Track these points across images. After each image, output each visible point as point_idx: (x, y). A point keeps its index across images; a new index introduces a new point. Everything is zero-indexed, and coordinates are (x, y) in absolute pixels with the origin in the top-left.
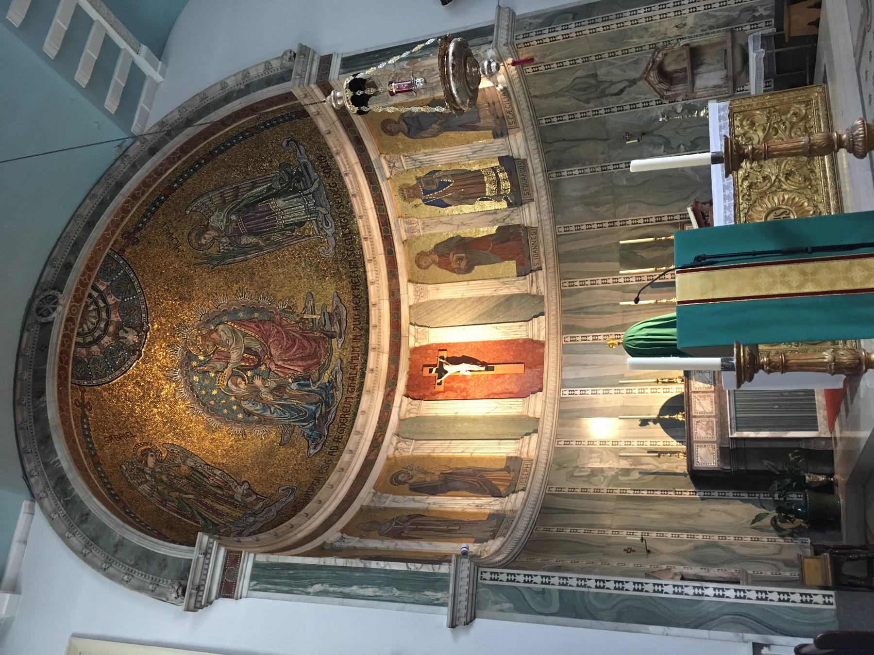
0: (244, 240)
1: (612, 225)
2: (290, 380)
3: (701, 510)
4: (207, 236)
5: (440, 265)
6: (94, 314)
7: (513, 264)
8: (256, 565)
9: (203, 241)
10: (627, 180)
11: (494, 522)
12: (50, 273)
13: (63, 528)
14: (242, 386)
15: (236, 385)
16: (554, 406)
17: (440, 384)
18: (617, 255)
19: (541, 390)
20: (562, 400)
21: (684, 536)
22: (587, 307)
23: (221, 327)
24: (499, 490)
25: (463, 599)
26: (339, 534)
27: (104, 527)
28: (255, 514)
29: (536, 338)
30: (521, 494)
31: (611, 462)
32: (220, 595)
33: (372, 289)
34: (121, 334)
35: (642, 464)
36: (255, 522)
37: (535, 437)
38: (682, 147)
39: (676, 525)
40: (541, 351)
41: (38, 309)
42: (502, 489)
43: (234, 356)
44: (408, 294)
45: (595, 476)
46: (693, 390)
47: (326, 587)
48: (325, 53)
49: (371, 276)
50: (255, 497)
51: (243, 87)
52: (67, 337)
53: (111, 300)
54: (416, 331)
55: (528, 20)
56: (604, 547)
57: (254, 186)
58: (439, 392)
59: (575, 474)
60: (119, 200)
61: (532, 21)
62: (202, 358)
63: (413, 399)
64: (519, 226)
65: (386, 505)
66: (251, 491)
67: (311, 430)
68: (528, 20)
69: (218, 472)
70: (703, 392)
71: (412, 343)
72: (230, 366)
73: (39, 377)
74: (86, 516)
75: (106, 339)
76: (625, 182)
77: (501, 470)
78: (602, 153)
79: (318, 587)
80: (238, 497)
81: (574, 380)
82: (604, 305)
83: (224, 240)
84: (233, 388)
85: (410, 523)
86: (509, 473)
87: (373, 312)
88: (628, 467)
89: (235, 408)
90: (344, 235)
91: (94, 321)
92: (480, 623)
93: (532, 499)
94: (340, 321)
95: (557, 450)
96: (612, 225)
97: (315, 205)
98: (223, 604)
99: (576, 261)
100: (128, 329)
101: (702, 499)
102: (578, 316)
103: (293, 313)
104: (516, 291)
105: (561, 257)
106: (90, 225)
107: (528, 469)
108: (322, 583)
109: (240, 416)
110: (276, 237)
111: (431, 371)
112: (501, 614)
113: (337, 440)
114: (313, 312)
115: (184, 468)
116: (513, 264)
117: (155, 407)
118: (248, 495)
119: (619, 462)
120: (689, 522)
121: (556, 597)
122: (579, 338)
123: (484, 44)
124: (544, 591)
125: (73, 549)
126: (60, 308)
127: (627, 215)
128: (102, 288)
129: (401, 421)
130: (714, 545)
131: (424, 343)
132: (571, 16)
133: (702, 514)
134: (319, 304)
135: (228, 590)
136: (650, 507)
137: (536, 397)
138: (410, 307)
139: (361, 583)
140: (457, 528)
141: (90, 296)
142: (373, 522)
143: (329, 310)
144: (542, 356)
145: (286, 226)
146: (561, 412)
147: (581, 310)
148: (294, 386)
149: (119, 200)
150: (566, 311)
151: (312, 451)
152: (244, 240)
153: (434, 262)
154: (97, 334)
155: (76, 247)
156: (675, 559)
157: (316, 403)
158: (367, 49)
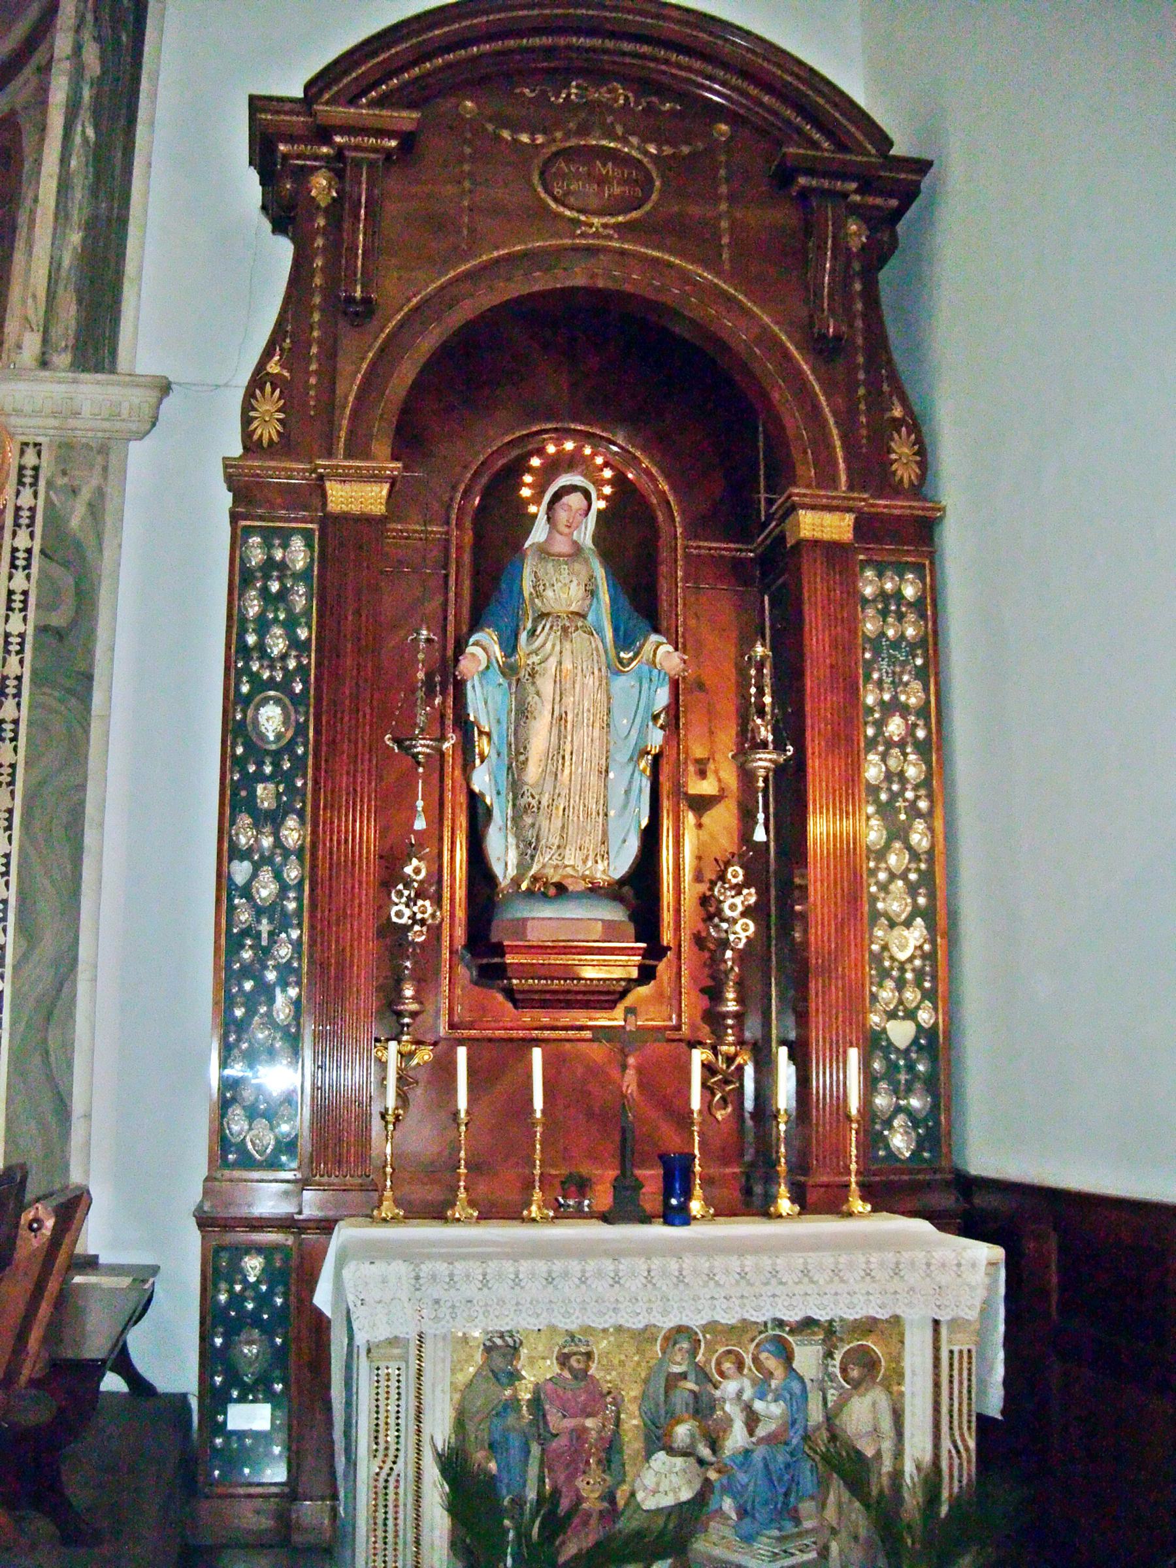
61: (86, 494)
68: (95, 482)
123: (45, 341)
132: (57, 620)
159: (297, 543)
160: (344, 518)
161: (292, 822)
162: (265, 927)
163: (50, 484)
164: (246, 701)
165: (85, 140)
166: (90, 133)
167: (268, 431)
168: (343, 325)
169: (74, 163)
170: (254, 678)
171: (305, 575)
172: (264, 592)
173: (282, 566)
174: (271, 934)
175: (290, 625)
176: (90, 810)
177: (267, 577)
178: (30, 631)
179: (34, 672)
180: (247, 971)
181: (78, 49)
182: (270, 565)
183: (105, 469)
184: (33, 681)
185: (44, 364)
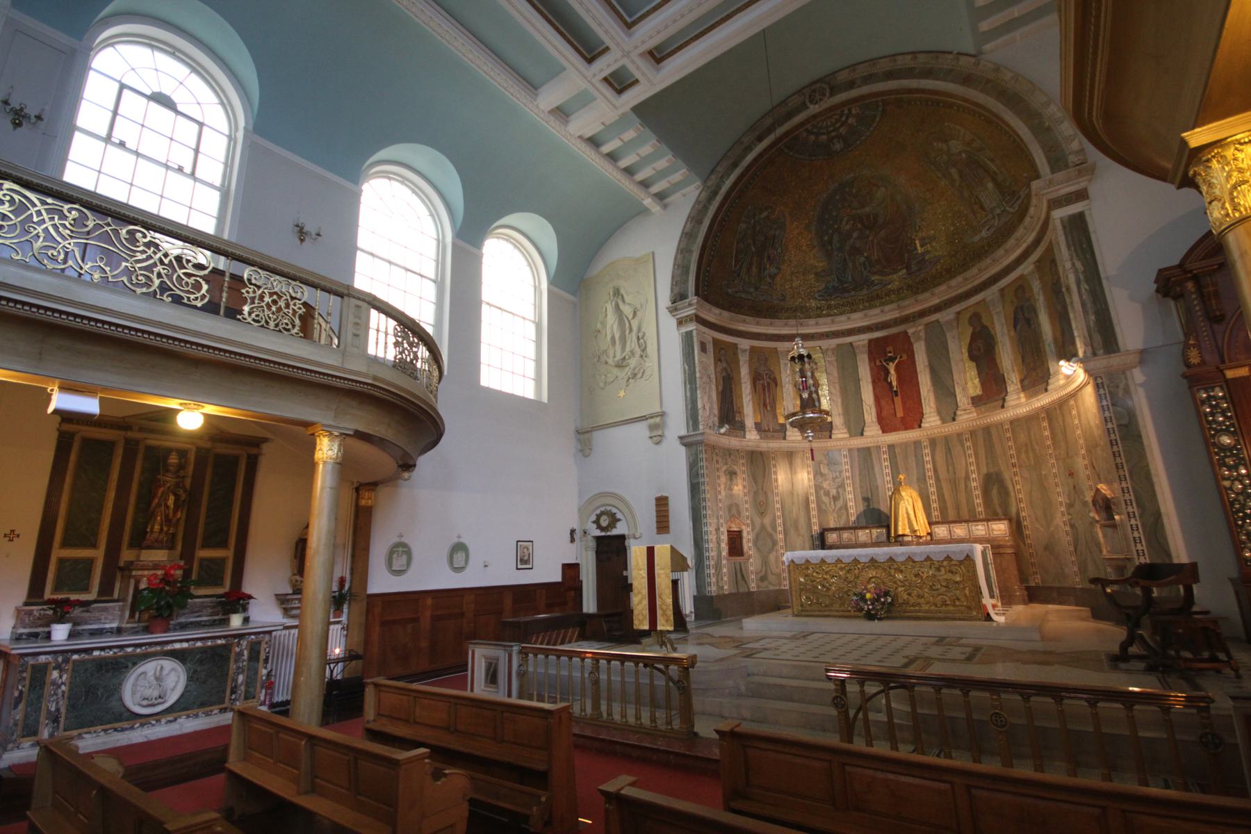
0: (953, 171)
1: (1014, 465)
2: (866, 254)
3: (803, 536)
4: (940, 144)
5: (973, 334)
6: (833, 121)
7: (979, 392)
8: (691, 331)
9: (935, 144)
10: (1045, 475)
12: (843, 77)
13: (692, 215)
14: (848, 227)
15: (847, 223)
17: (881, 362)
18: (992, 471)
19: (883, 432)
20: (878, 448)
21: (780, 529)
22: (951, 453)
23: (883, 189)
25: (687, 440)
26: (748, 348)
27: (696, 237)
28: (756, 289)
29: (923, 420)
30: (800, 438)
32: (677, 319)
33: (943, 288)
34: (835, 141)
35: (834, 501)
36: (751, 293)
37: (847, 435)
38: (1070, 517)
40: (916, 426)
41: (814, 91)
43: (867, 209)
44: (946, 316)
47: (687, 372)
48: (1092, 191)
49: (953, 282)
50: (770, 281)
51: (1047, 124)
52: (802, 124)
53: (850, 121)
54: (920, 331)
55: (1125, 381)
56: (762, 489)
57: (992, 160)
58: (875, 363)
60: (913, 83)
62: (854, 191)
63: (869, 347)
64: (1007, 392)
65: (781, 361)
66: (773, 277)
67: (833, 287)
69: (779, 251)
71: (910, 331)
72: (858, 211)
73: (771, 129)
74: (700, 222)
75: (825, 137)
76: (1044, 473)
78: (1060, 454)
79: (687, 367)
80: (767, 272)
81: (895, 452)
83: (945, 156)
84: (844, 223)
85: (768, 380)
87: (927, 295)
88: (831, 494)
89: (830, 231)
90: (983, 247)
91: (829, 123)
92: (683, 449)
93: (797, 445)
94: (920, 270)
96: (1014, 465)
97: (998, 215)
98: (673, 322)
99: (985, 441)
100: (841, 141)
101: (812, 536)
103: (917, 232)
104: (958, 400)
105: (987, 430)
106: (890, 75)
108: (689, 370)
109: (826, 238)
110: (966, 194)
111: (890, 352)
112: (688, 458)
113: (829, 307)
114: (922, 246)
115: (772, 232)
116: (979, 392)
117: (803, 190)
118: (770, 276)
120: (792, 532)
121: (696, 481)
122: (927, 451)
123: (1093, 348)
124: (698, 475)
125: (685, 227)
126: (817, 106)
127: (1022, 477)
128: (854, 112)
129: (851, 343)
130: (775, 543)
131: (912, 340)
132: (1124, 422)
133: (800, 538)
134: (929, 247)
135: (680, 323)
138: (937, 321)
139: (691, 388)
140: (769, 408)
141: (843, 111)
142: (766, 359)
143: (926, 258)
144: (912, 428)
145: (977, 197)
146: (869, 449)
147: (949, 450)
148: (862, 259)
149: (913, 83)
150: (947, 439)
151: (816, 295)
152: (953, 171)
153: (975, 328)
154: (822, 131)
155: (869, 79)
157: (854, 280)
158: (1095, 232)
159: (1217, 389)
160: (1235, 380)
161: (1241, 467)
162: (1241, 498)
163: (1108, 387)
164: (1213, 436)
165: (1086, 290)
166: (1087, 287)
167: (1194, 358)
168: (1216, 327)
169: (1084, 297)
170: (1215, 429)
171: (1223, 397)
172: (1211, 406)
173: (1215, 398)
174: (1245, 500)
175: (1223, 413)
176: (1153, 472)
177: (1210, 401)
178: (1115, 426)
179: (1120, 437)
180: (1239, 511)
181: (1073, 264)
182: (1209, 397)
183: (1126, 379)
184: (1121, 440)
185: (1094, 354)
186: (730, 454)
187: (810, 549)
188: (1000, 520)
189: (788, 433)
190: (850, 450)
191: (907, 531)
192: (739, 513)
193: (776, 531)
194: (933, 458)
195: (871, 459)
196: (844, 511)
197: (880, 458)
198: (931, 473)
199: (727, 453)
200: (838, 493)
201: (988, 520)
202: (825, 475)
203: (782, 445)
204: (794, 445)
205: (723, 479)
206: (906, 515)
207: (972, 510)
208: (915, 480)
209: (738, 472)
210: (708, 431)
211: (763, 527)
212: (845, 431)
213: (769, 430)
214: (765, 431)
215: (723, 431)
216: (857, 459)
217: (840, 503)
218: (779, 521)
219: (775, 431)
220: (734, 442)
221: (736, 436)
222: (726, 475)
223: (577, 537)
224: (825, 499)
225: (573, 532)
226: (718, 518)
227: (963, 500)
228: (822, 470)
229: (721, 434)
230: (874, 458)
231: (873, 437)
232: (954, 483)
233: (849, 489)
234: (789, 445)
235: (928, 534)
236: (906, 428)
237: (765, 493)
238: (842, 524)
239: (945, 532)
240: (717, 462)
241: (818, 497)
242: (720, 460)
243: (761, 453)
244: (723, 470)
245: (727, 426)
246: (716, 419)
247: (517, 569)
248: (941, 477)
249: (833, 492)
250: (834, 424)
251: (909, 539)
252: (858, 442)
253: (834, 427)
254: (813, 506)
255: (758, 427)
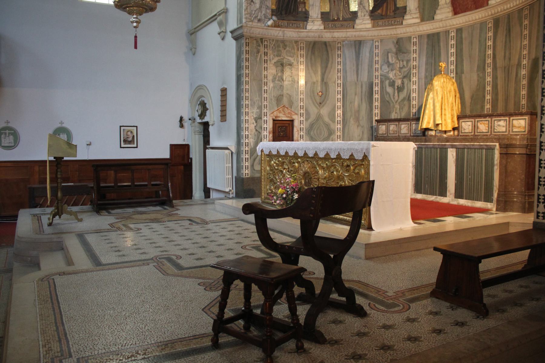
3: (362, 127)
11: (349, 16)
16: (440, 28)
20: (447, 32)
22: (510, 35)
24: (378, 10)
30: (370, 26)
31: (400, 74)
35: (398, 93)
37: (418, 21)
39: (348, 114)
42: (379, 11)
45: (388, 67)
46: (412, 123)
59: (390, 55)
70: (411, 129)
77: (395, 5)
81: (462, 38)
82: (510, 49)
86: (393, 11)
88: (396, 85)
92: (234, 42)
95: (409, 38)
101: (372, 127)
102: (505, 28)
107: (396, 23)
119: (400, 79)
120: (352, 121)
136: (363, 100)
137: (449, 12)
146: (438, 34)
156: (313, 117)
186: (285, 47)
187: (368, 140)
188: (522, 114)
189: (357, 21)
190: (420, 37)
191: (431, 126)
192: (291, 103)
193: (334, 122)
194: (494, 42)
195: (439, 46)
196: (406, 102)
197: (447, 44)
198: (489, 61)
199: (281, 45)
200: (403, 83)
201: (511, 115)
202: (392, 64)
203: (349, 34)
204: (361, 33)
205: (272, 71)
206: (432, 107)
207: (517, 104)
208: (476, 69)
209: (295, 63)
210: (255, 24)
211: (319, 117)
212: (418, 15)
213: (338, 19)
214: (334, 20)
215: (270, 23)
216: (425, 46)
217: (403, 95)
218: (339, 112)
219: (345, 20)
220: (290, 33)
221: (297, 27)
222: (277, 67)
223: (185, 124)
224: (389, 90)
225: (181, 119)
226: (260, 108)
227: (512, 92)
228: (390, 60)
229: (269, 26)
230: (442, 44)
231: (441, 20)
232: (507, 70)
233: (414, 79)
234: (357, 33)
235: (454, 129)
236: (477, 8)
237: (326, 84)
238: (403, 115)
239: (470, 127)
240: (266, 54)
241: (382, 88)
242: (270, 52)
243: (325, 43)
244: (273, 62)
245: (274, 18)
246: (269, 12)
247: (121, 147)
248: (498, 65)
249: (399, 82)
250: (408, 9)
251: (433, 133)
252: (428, 28)
253: (407, 13)
254: (376, 96)
255: (325, 17)
